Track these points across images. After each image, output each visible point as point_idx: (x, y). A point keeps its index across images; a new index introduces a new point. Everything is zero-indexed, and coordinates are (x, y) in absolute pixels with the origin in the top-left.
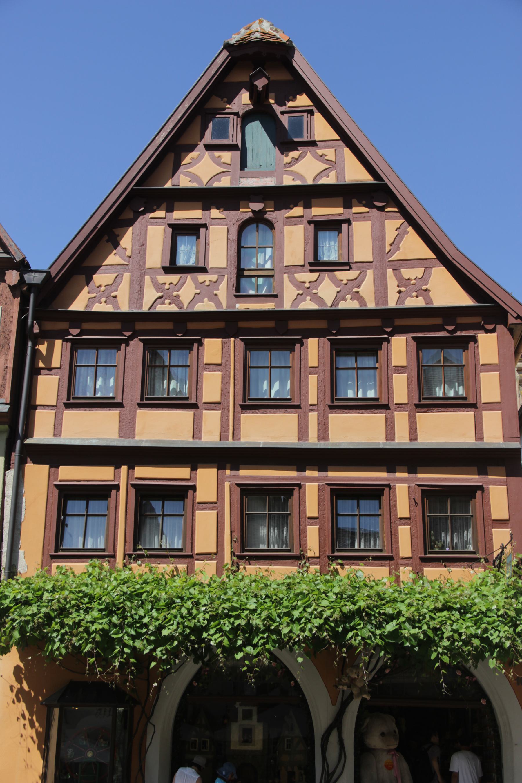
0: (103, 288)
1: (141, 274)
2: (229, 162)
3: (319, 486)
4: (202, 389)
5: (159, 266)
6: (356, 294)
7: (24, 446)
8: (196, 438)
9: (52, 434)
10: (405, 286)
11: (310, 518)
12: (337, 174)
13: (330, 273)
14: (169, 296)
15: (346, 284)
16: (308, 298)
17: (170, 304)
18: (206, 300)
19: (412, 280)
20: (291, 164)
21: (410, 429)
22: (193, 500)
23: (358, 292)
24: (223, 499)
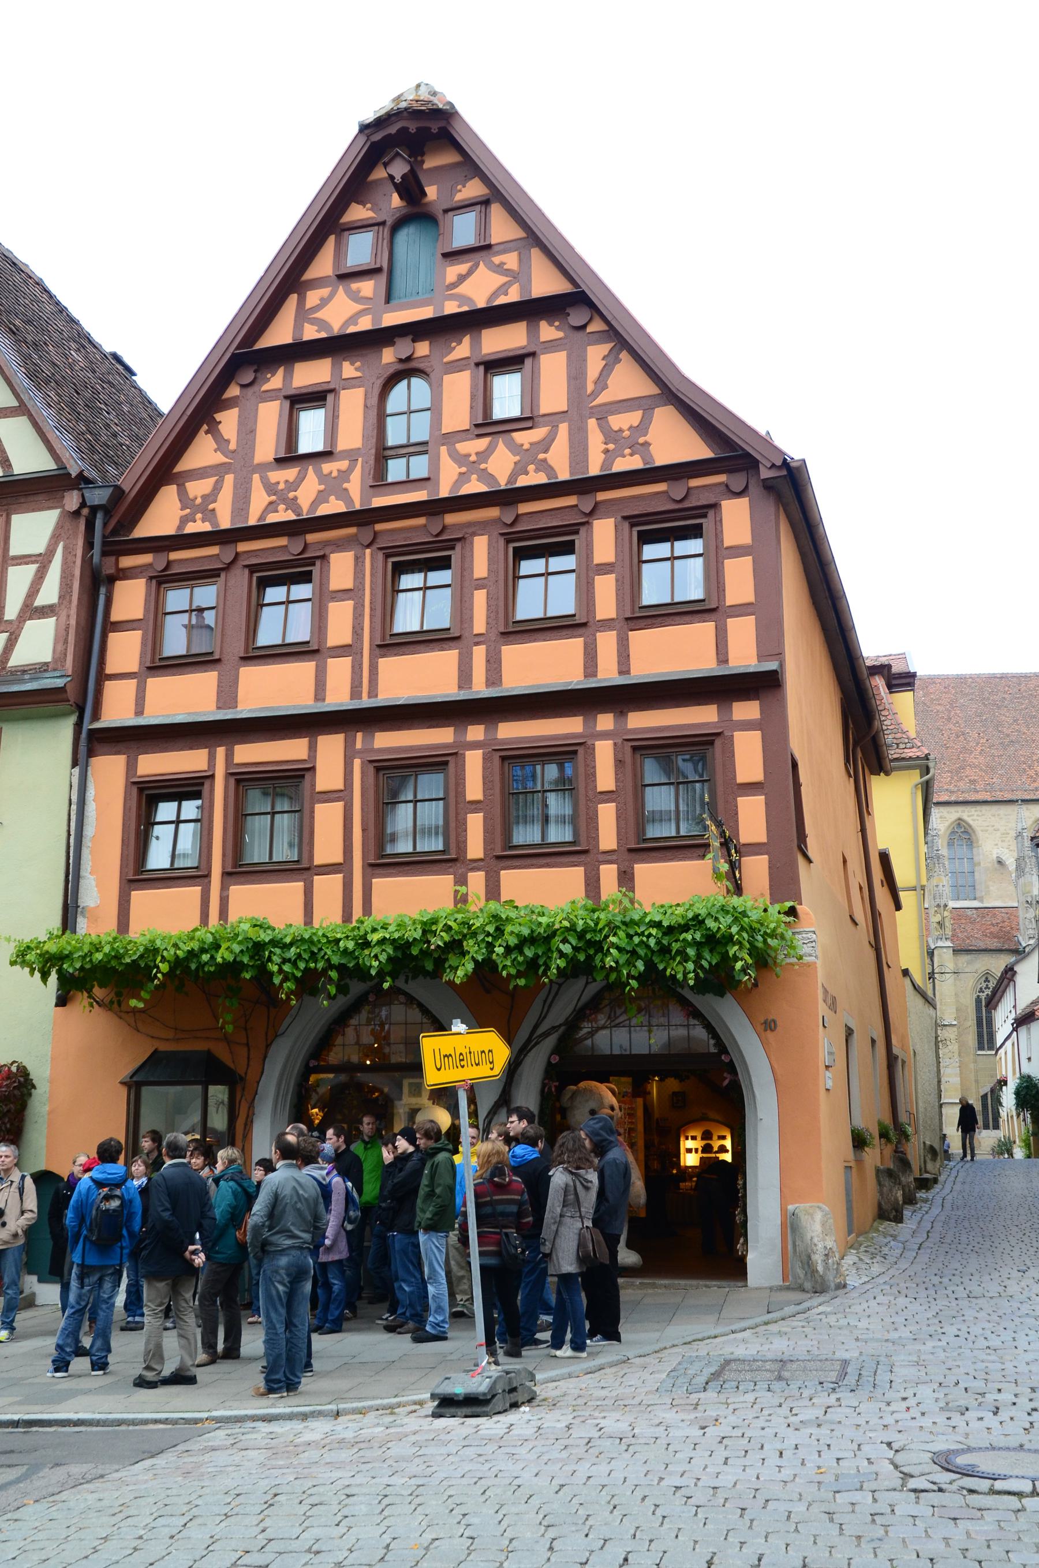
10: (615, 441)
11: (472, 802)
12: (522, 288)
13: (506, 436)
14: (284, 499)
15: (527, 450)
16: (474, 477)
18: (332, 498)
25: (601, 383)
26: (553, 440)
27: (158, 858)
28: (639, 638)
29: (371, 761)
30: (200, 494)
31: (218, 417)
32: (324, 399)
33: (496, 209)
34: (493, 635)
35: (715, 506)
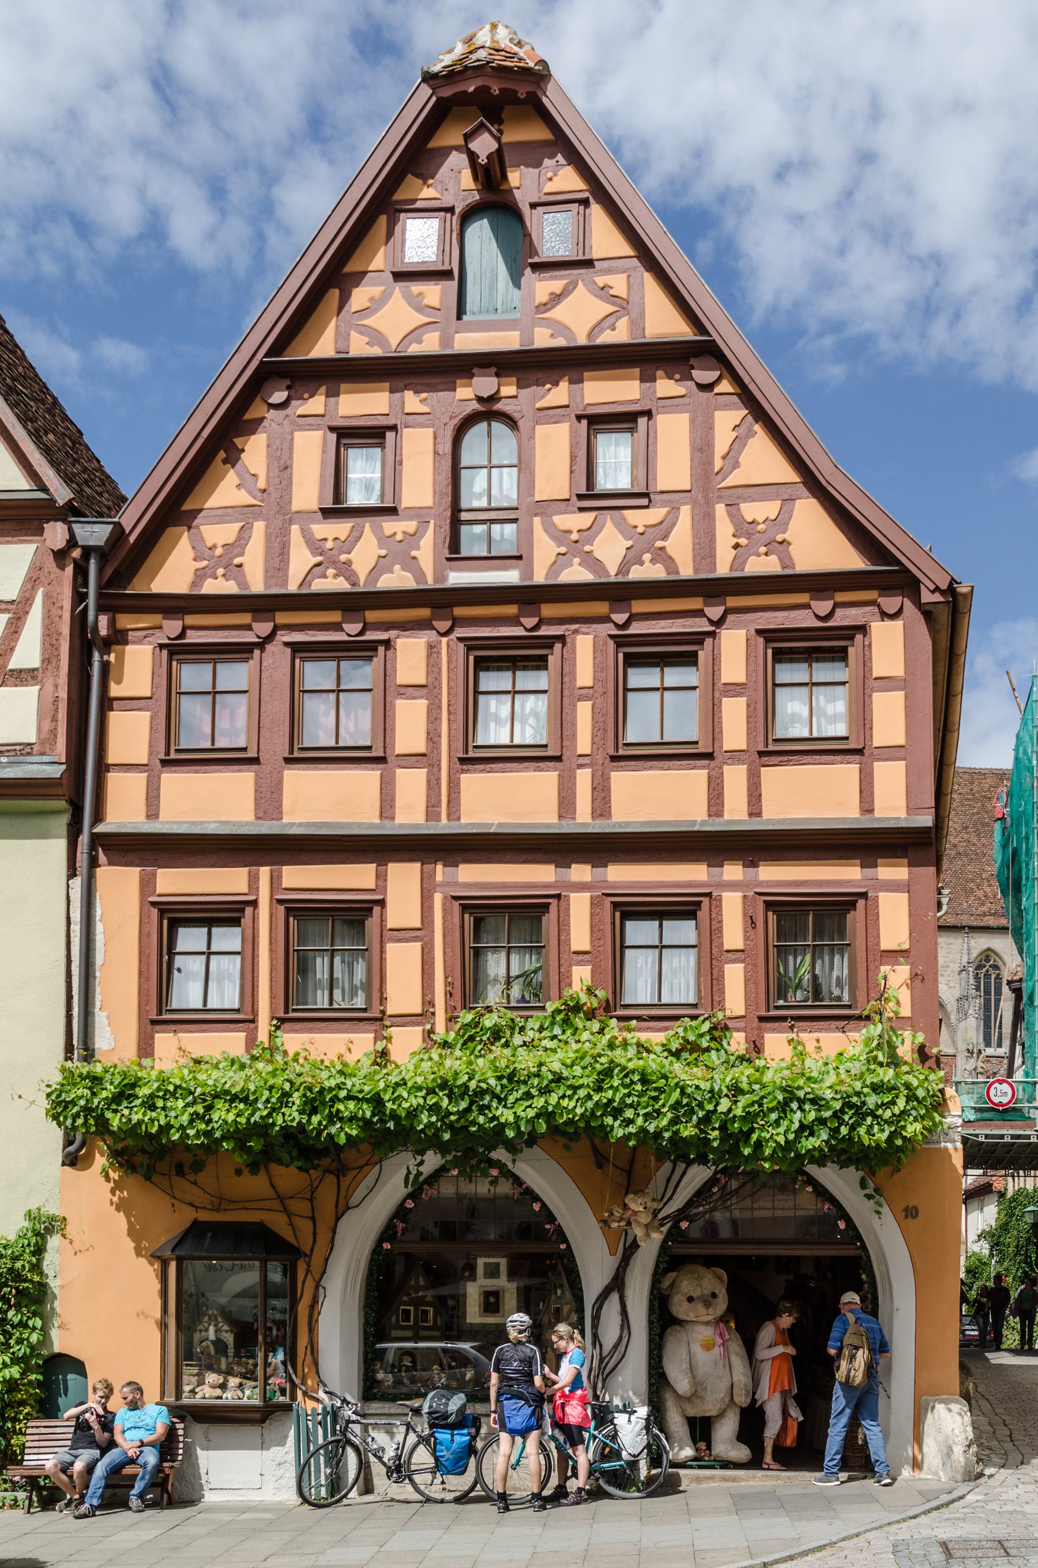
0: (219, 551)
1: (284, 520)
2: (437, 305)
3: (592, 897)
4: (393, 730)
5: (315, 506)
6: (660, 552)
7: (96, 839)
8: (386, 818)
9: (144, 814)
10: (749, 535)
14: (334, 563)
15: (642, 534)
16: (577, 560)
17: (335, 576)
18: (397, 567)
19: (759, 524)
20: (549, 306)
21: (750, 795)
22: (382, 926)
23: (662, 549)
24: (432, 922)
25: (732, 458)
26: (673, 525)
27: (187, 993)
28: (772, 776)
29: (456, 898)
30: (220, 543)
31: (238, 441)
32: (383, 436)
33: (596, 211)
34: (599, 758)
35: (863, 629)
